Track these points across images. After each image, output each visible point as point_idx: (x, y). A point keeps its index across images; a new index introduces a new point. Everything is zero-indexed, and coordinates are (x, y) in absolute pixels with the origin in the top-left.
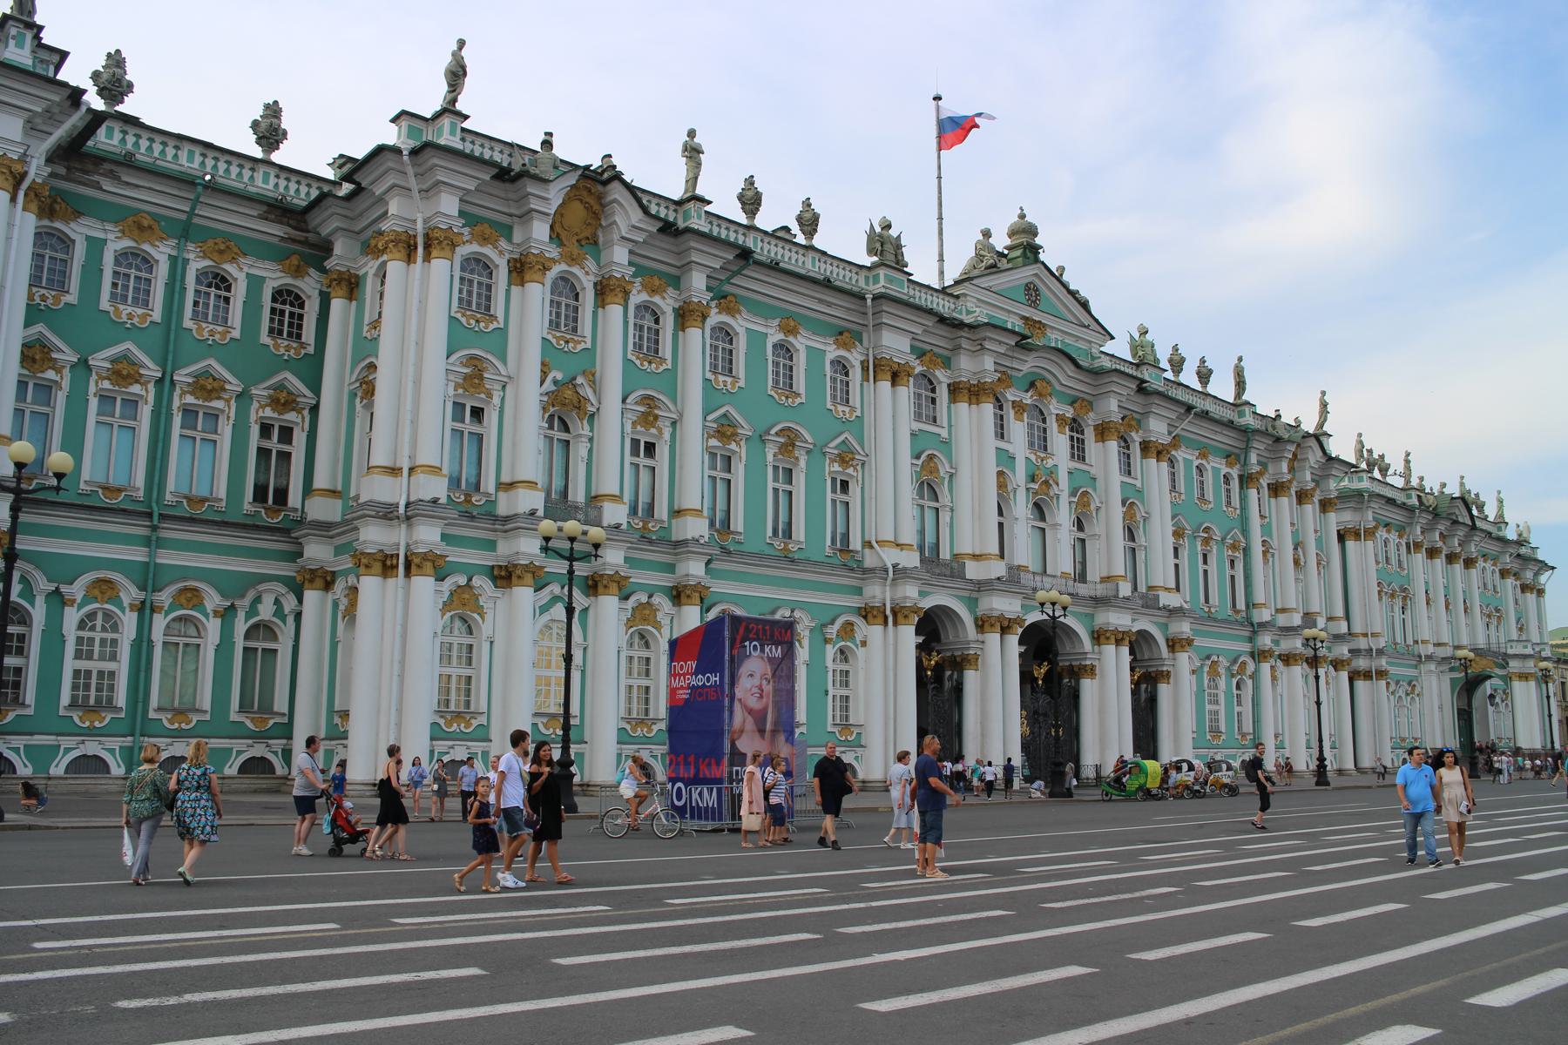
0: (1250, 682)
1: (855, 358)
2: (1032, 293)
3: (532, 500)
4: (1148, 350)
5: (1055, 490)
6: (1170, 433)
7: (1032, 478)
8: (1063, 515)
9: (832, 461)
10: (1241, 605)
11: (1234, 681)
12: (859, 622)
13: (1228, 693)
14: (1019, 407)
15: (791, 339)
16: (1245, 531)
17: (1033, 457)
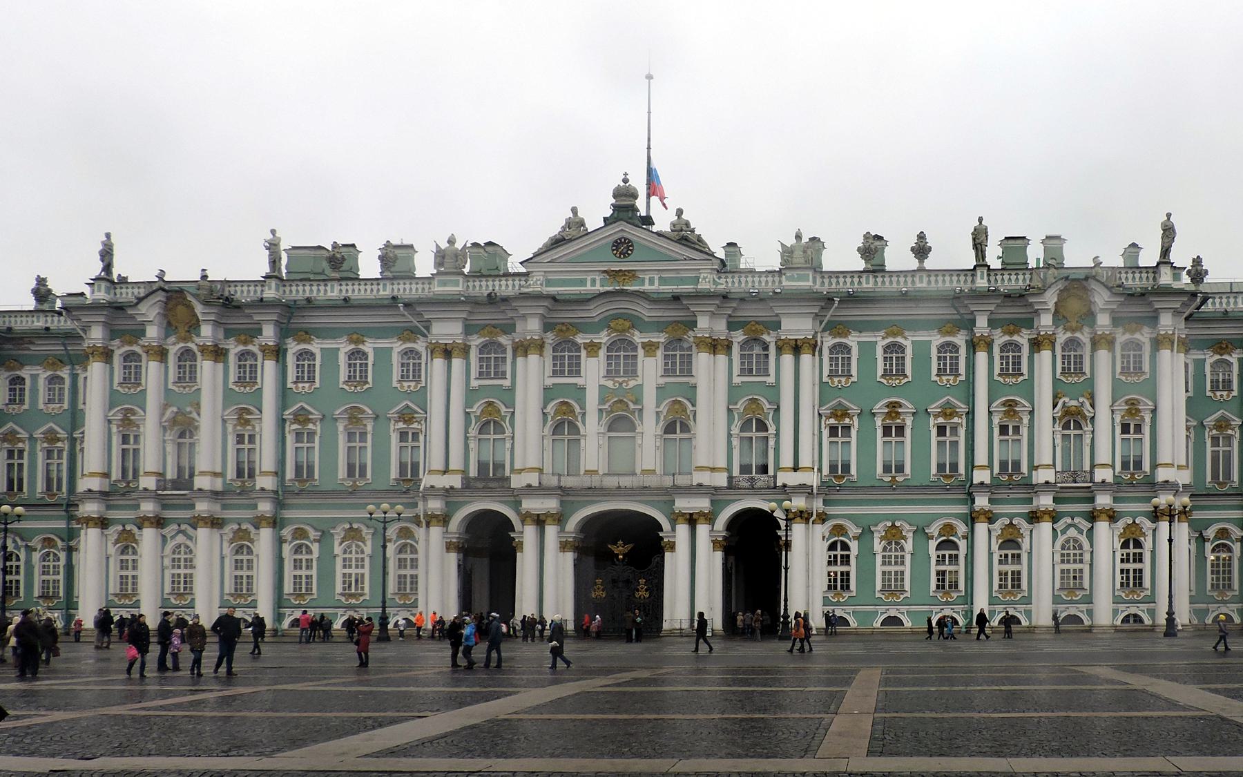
0: (962, 544)
1: (420, 346)
2: (622, 247)
3: (148, 483)
4: (798, 253)
5: (632, 406)
6: (821, 322)
7: (602, 401)
8: (649, 427)
9: (397, 422)
10: (962, 469)
11: (933, 545)
12: (413, 527)
13: (920, 557)
14: (593, 348)
15: (361, 346)
16: (970, 399)
17: (610, 384)
